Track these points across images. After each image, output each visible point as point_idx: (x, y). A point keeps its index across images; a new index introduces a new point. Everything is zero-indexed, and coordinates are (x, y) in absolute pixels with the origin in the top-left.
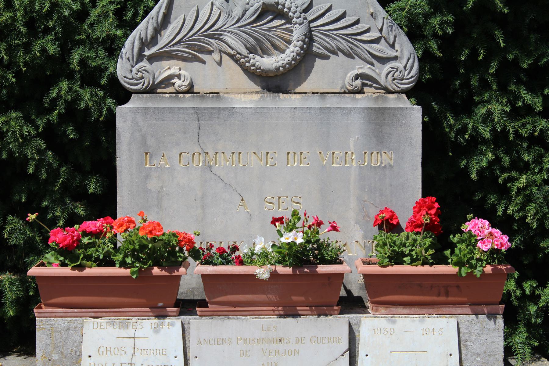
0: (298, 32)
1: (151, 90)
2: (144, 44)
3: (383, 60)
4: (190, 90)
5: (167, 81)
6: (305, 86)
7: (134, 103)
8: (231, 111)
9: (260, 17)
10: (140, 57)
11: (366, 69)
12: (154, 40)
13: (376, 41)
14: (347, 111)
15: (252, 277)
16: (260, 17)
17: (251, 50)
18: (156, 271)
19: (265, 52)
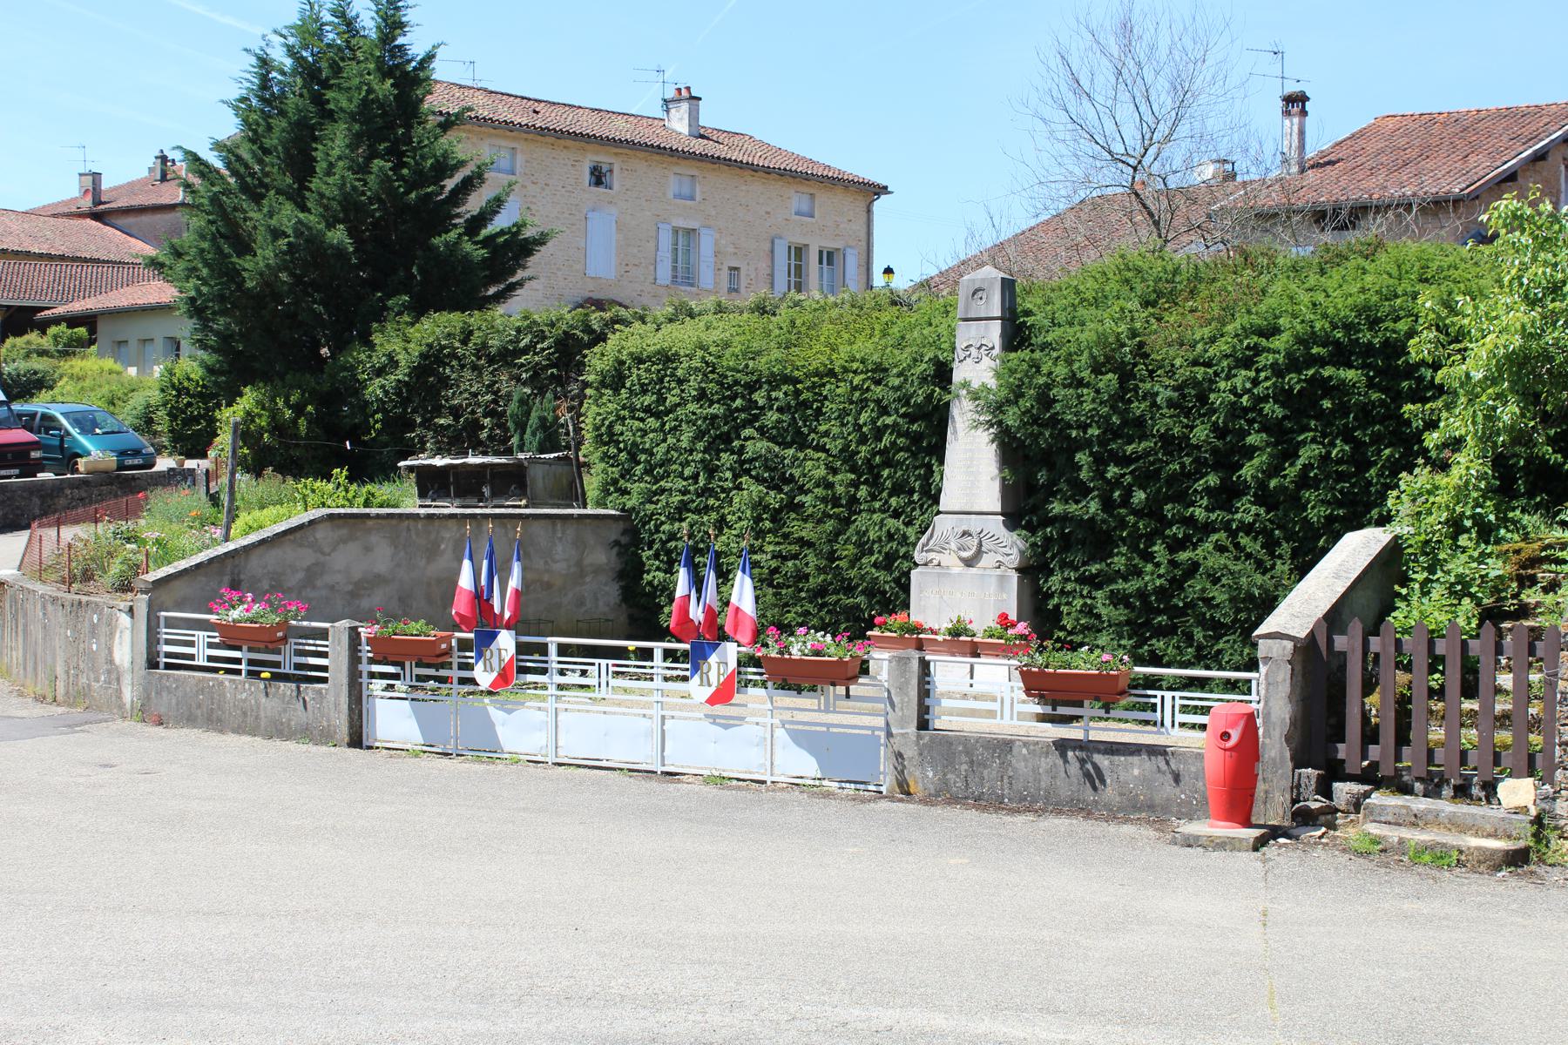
0: (976, 541)
1: (926, 565)
2: (924, 546)
3: (1008, 555)
5: (931, 561)
7: (919, 569)
11: (1001, 559)
12: (927, 544)
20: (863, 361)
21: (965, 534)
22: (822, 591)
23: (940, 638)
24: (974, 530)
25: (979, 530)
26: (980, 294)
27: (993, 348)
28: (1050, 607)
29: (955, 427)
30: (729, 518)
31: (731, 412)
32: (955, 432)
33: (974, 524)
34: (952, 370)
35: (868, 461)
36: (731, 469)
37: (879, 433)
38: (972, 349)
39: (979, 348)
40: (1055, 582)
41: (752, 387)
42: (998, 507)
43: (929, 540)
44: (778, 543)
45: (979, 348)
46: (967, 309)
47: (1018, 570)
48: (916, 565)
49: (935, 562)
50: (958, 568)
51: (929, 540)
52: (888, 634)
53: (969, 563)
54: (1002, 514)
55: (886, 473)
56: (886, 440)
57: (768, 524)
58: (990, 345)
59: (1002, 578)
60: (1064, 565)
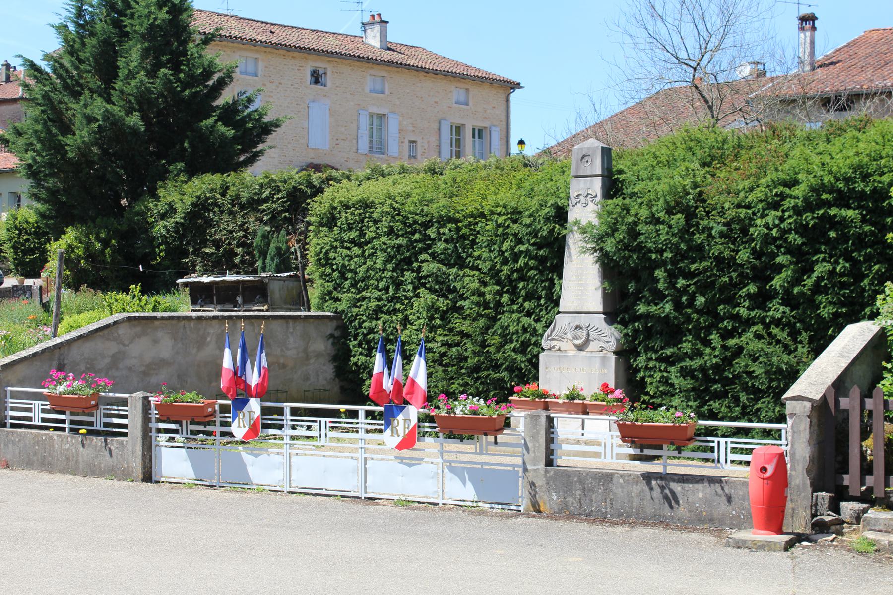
0: (585, 333)
1: (550, 349)
2: (548, 336)
3: (608, 342)
4: (559, 349)
5: (554, 347)
6: (588, 349)
8: (567, 356)
9: (576, 328)
10: (547, 340)
11: (603, 345)
12: (551, 335)
13: (606, 336)
14: (596, 357)
15: (557, 402)
16: (576, 328)
17: (574, 338)
18: (537, 399)
19: (577, 339)
20: (504, 207)
21: (578, 327)
22: (477, 369)
23: (560, 401)
24: (584, 324)
25: (587, 325)
26: (586, 158)
27: (596, 196)
28: (638, 378)
29: (569, 253)
30: (411, 317)
31: (411, 242)
32: (570, 256)
33: (584, 320)
34: (567, 212)
35: (508, 277)
36: (412, 283)
37: (516, 257)
38: (581, 197)
39: (586, 197)
40: (641, 361)
41: (427, 225)
42: (600, 309)
43: (552, 332)
44: (446, 335)
45: (586, 197)
46: (577, 168)
47: (615, 352)
48: (543, 349)
49: (557, 347)
50: (573, 352)
51: (552, 332)
52: (524, 398)
53: (580, 348)
54: (604, 313)
55: (521, 285)
56: (521, 262)
57: (438, 322)
58: (594, 195)
59: (604, 359)
60: (647, 349)
